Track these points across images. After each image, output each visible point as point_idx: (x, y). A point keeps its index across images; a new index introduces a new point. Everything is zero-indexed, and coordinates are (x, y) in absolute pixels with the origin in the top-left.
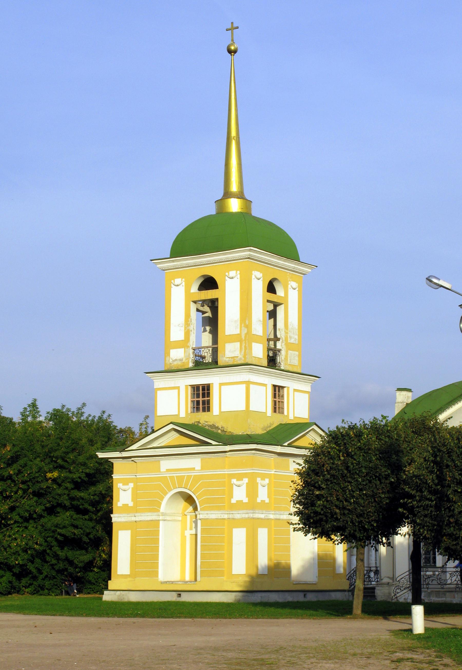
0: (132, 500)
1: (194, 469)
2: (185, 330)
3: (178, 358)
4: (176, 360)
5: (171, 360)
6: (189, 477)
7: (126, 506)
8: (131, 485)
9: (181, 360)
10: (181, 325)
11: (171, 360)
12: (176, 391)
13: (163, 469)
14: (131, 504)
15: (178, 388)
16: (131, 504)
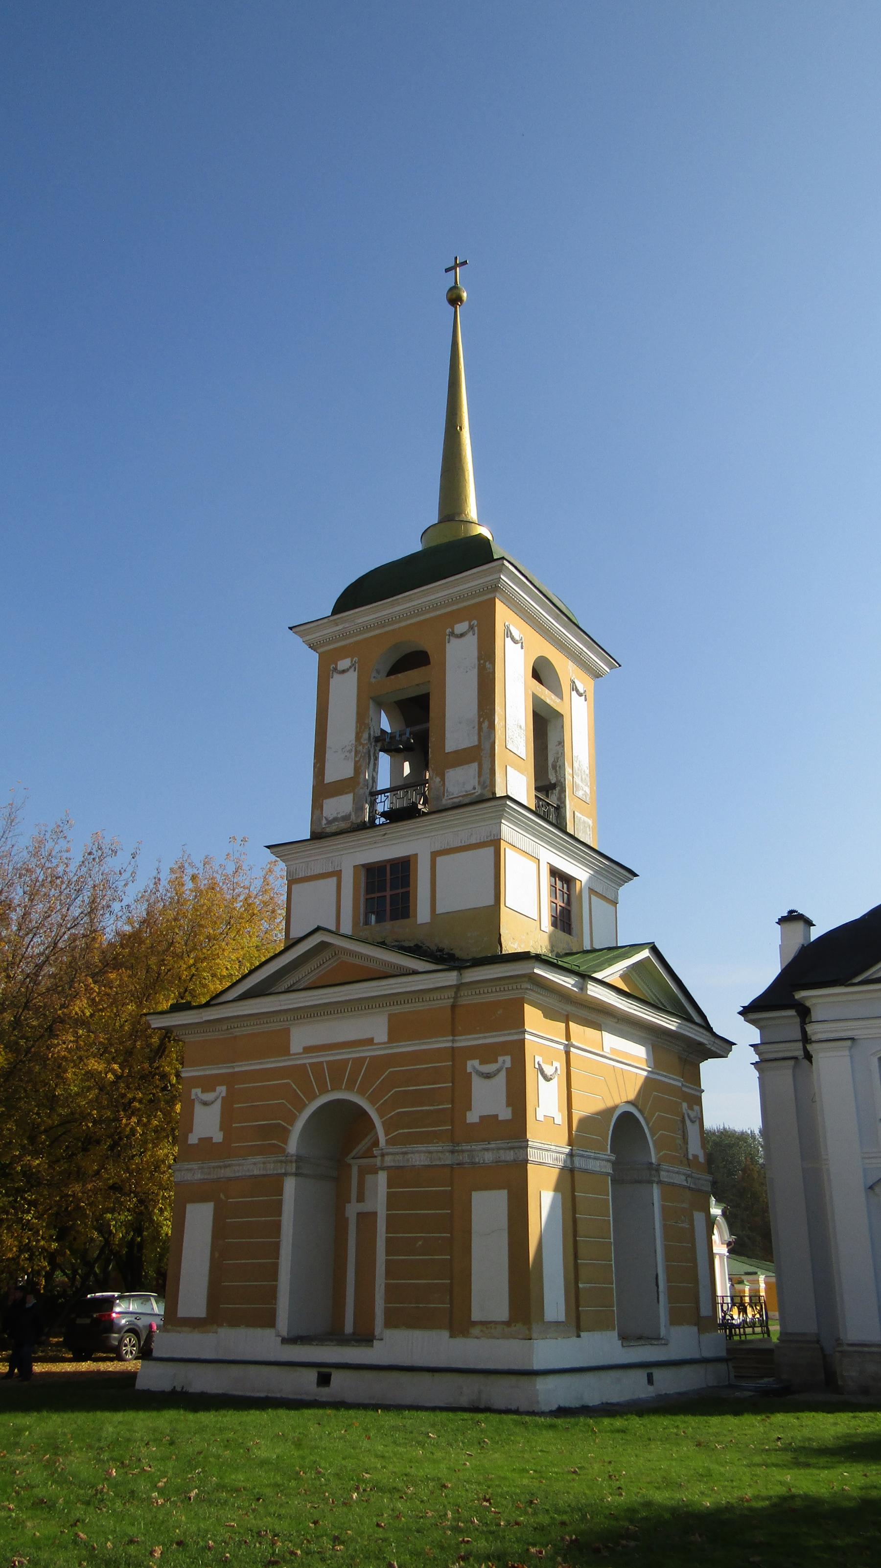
0: (222, 1129)
1: (370, 1041)
2: (356, 756)
3: (339, 816)
4: (335, 820)
5: (324, 822)
6: (359, 1061)
7: (206, 1141)
8: (222, 1090)
9: (346, 818)
10: (349, 748)
11: (324, 822)
12: (335, 879)
13: (296, 1046)
14: (218, 1137)
15: (338, 874)
16: (218, 1137)
